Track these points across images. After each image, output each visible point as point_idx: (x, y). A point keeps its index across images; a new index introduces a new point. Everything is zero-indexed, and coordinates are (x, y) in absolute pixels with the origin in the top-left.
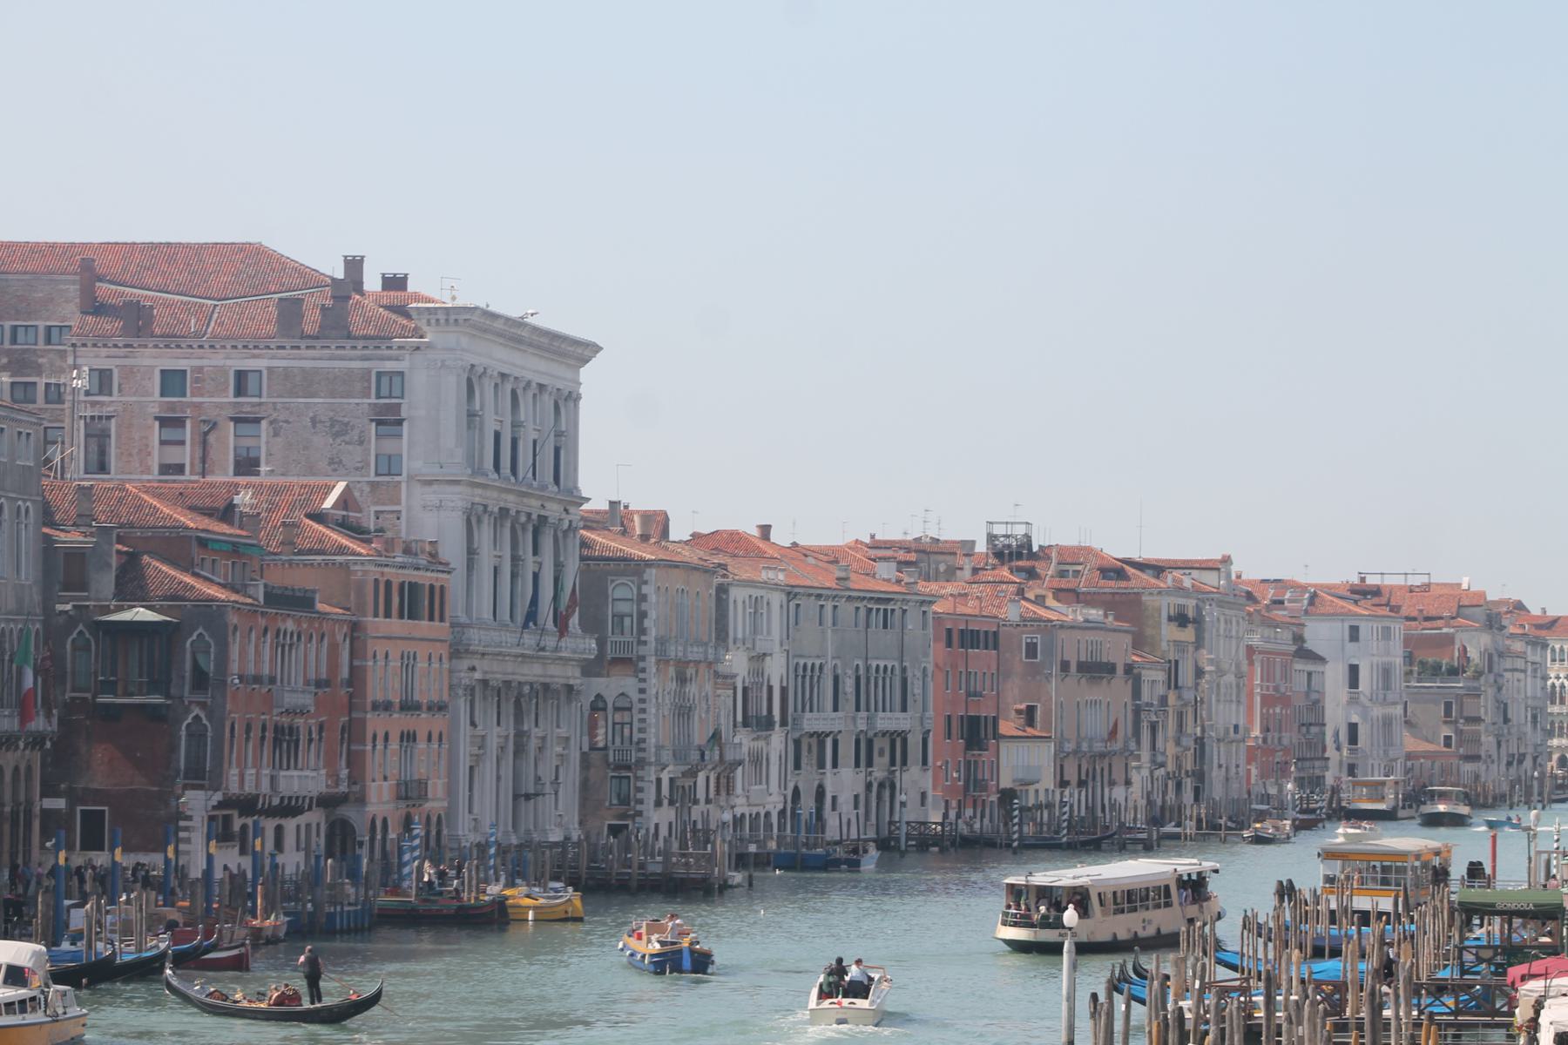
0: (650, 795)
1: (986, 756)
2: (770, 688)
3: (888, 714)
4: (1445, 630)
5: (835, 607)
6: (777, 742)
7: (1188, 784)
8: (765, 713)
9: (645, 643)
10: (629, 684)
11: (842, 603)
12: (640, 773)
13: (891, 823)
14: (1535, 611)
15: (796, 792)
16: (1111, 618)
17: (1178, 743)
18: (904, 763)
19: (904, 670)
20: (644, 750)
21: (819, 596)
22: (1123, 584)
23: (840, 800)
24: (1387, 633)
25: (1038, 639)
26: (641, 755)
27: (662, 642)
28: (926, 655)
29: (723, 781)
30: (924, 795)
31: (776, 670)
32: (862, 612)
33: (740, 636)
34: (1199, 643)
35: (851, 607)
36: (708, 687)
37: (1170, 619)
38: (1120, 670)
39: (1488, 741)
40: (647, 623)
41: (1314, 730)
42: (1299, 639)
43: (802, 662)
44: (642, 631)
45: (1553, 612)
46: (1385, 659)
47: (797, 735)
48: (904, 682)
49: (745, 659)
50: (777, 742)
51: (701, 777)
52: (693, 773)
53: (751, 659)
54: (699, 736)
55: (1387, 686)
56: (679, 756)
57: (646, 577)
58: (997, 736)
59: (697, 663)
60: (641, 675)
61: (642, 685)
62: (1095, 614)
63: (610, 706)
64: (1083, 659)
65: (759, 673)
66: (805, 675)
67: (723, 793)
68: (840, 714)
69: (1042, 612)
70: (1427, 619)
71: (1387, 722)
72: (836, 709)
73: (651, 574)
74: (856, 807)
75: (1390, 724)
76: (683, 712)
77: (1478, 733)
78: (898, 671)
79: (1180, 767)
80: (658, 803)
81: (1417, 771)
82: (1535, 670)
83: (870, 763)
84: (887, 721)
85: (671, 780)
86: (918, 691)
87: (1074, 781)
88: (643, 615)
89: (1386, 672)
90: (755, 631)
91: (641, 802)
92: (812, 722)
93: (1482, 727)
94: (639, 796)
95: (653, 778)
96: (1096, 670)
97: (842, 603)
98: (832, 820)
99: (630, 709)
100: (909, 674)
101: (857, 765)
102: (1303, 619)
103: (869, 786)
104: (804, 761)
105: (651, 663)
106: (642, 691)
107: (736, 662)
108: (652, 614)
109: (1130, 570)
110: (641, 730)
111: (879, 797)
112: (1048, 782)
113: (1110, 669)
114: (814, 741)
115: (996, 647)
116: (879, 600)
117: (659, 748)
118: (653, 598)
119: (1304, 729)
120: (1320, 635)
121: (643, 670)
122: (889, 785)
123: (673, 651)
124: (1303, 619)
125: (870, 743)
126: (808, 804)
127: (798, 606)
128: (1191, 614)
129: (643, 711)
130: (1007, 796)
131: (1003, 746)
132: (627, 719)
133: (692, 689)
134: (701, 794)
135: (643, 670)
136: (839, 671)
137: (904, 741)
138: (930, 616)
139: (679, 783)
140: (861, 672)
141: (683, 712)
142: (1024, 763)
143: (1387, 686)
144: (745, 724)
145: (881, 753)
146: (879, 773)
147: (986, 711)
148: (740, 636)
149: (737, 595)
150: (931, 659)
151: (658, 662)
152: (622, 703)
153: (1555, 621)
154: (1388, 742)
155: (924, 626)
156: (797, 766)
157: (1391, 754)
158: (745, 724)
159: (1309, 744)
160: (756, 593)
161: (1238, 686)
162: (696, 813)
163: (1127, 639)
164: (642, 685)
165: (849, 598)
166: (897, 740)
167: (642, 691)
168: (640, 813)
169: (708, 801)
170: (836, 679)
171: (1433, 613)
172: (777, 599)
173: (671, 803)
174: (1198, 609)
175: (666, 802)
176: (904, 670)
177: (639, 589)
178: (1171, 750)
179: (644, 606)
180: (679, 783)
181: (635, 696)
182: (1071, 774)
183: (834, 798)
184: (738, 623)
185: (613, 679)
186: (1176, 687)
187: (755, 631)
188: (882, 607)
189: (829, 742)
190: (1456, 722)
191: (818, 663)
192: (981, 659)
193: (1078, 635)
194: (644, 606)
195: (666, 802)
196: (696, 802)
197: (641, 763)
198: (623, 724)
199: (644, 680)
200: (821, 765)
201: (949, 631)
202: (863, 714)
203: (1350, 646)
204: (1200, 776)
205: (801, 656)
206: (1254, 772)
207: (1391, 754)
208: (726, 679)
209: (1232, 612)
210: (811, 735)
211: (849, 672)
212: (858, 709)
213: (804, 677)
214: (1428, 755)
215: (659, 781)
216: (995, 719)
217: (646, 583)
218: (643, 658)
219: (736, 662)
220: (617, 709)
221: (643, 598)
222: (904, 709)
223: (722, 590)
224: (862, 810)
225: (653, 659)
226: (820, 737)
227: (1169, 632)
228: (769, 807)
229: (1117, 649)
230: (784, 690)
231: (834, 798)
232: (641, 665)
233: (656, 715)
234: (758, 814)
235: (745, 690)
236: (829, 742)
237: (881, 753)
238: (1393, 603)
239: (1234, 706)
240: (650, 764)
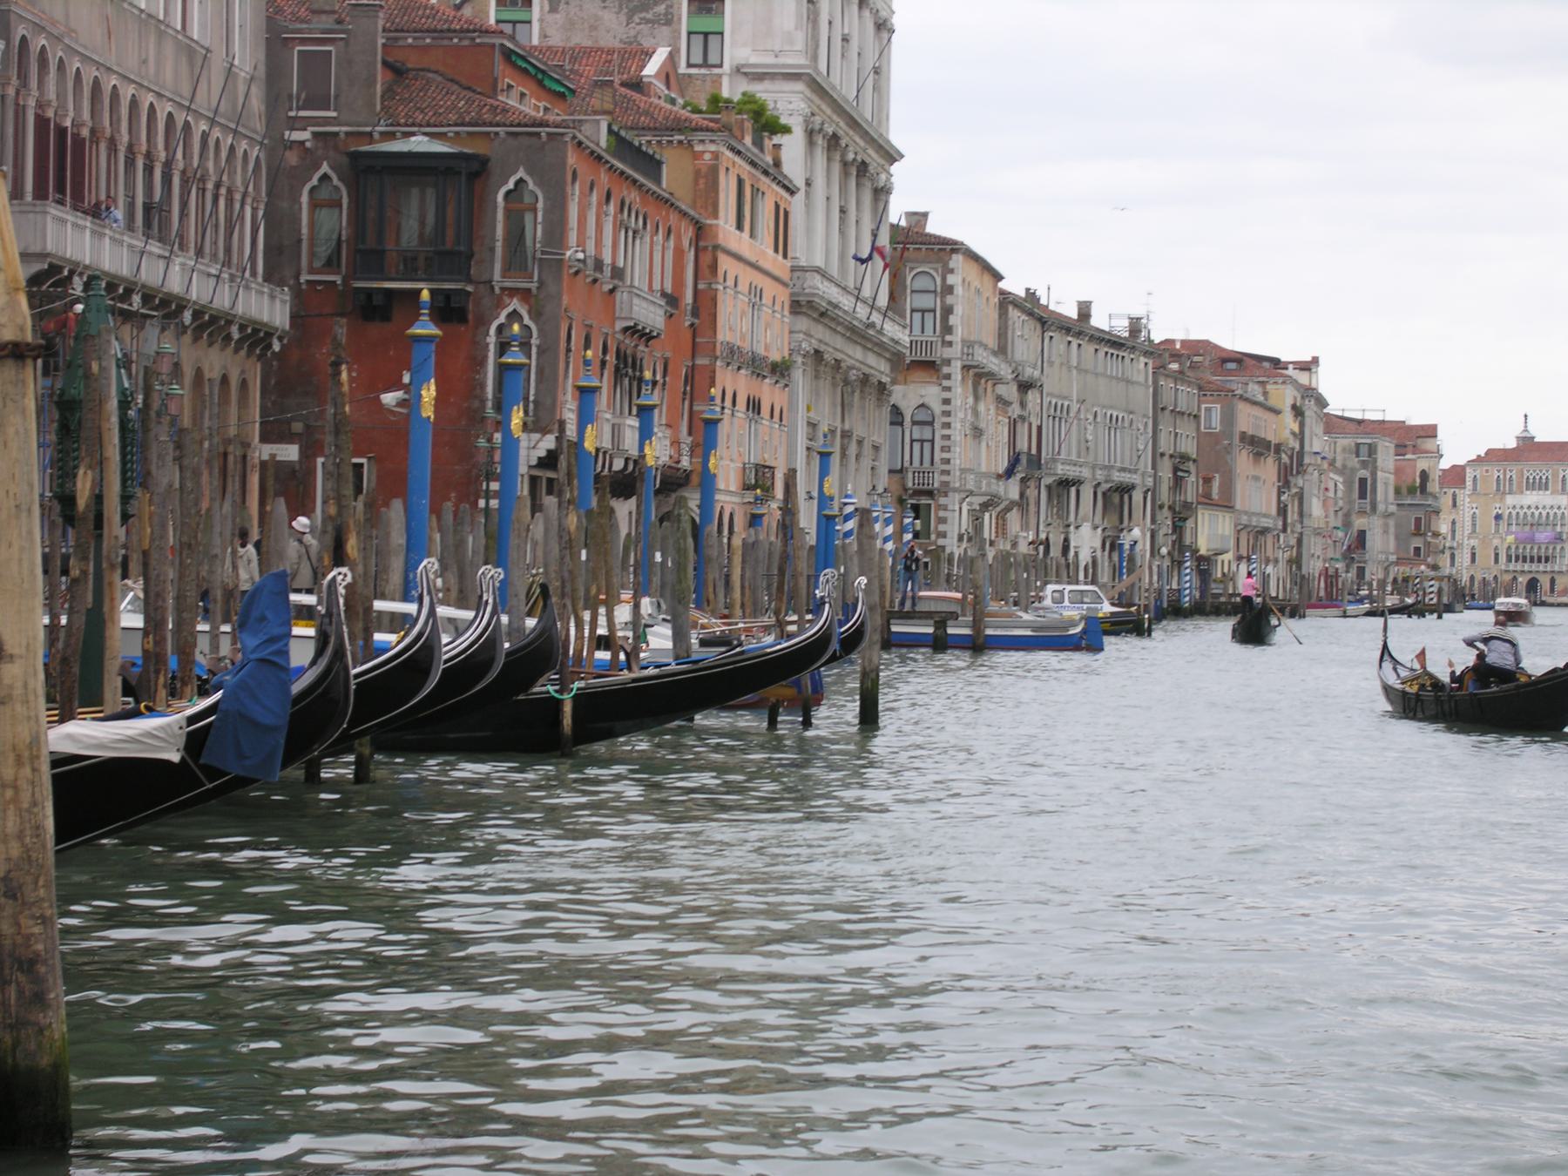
9: (950, 344)
10: (930, 393)
12: (942, 501)
26: (945, 478)
40: (953, 320)
44: (947, 329)
57: (952, 265)
60: (946, 383)
61: (946, 395)
63: (908, 420)
88: (948, 311)
91: (943, 535)
94: (941, 528)
99: (931, 424)
105: (955, 369)
106: (947, 402)
108: (959, 310)
110: (943, 449)
118: (959, 290)
121: (948, 377)
129: (947, 425)
132: (927, 435)
135: (948, 377)
152: (921, 417)
164: (946, 395)
167: (947, 402)
177: (944, 279)
179: (949, 300)
181: (937, 408)
185: (912, 387)
194: (949, 300)
197: (945, 489)
198: (922, 441)
199: (948, 389)
217: (952, 271)
218: (948, 362)
220: (914, 423)
221: (949, 290)
232: (945, 370)
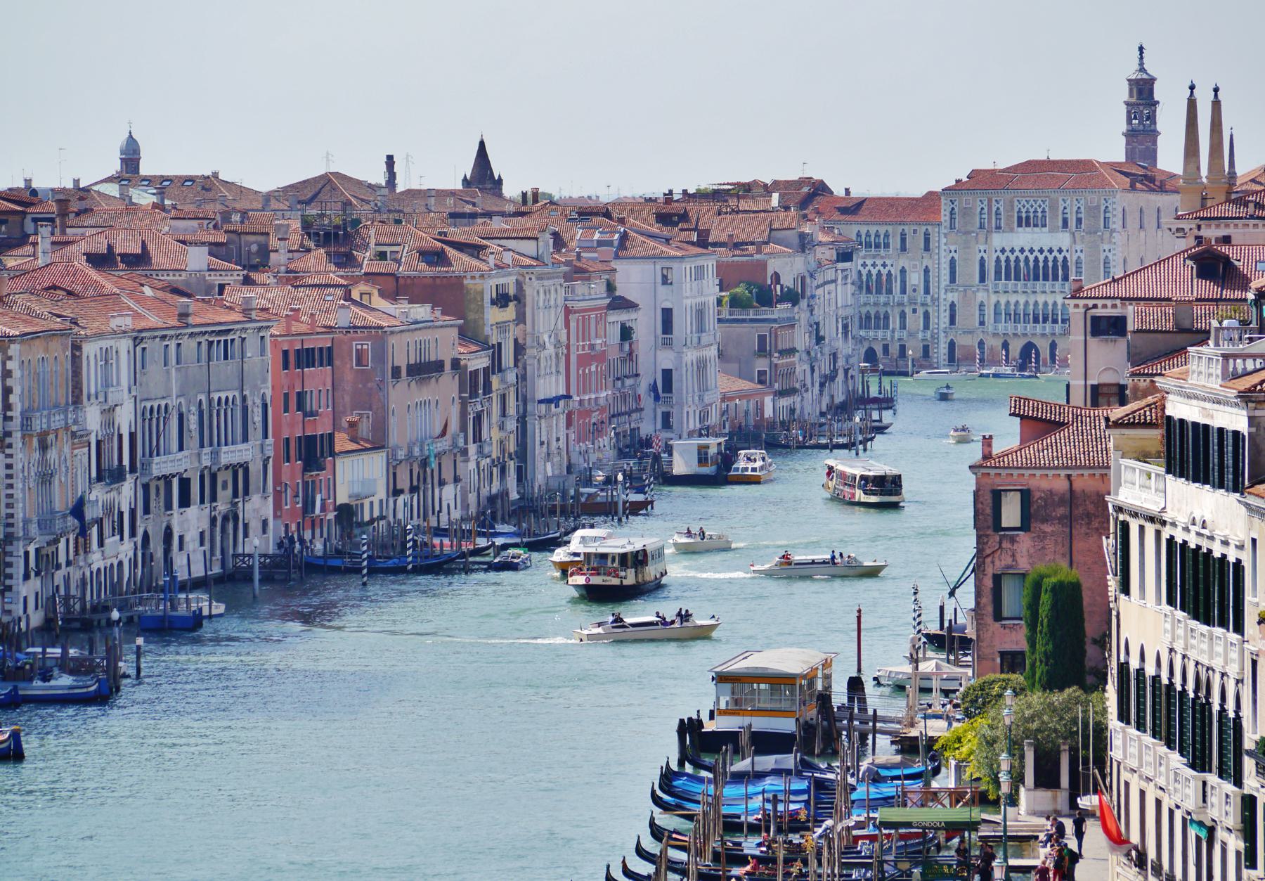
0: (18, 570)
1: (323, 475)
2: (120, 436)
3: (231, 448)
4: (757, 257)
5: (179, 345)
6: (126, 494)
7: (512, 466)
8: (116, 462)
9: (11, 418)
11: (185, 341)
13: (235, 556)
14: (839, 191)
15: (146, 536)
16: (438, 313)
17: (502, 428)
18: (246, 492)
19: (244, 398)
20: (12, 525)
21: (163, 337)
22: (440, 270)
23: (187, 539)
24: (700, 273)
25: (367, 346)
27: (26, 419)
28: (264, 381)
29: (81, 540)
30: (265, 523)
31: (125, 419)
32: (204, 346)
33: (93, 391)
34: (521, 318)
35: (193, 343)
36: (67, 449)
37: (493, 303)
38: (448, 366)
39: (802, 368)
40: (13, 399)
41: (629, 382)
42: (610, 287)
43: (148, 405)
45: (857, 193)
46: (699, 300)
47: (145, 480)
48: (245, 409)
49: (98, 412)
50: (126, 494)
51: (63, 540)
52: (56, 541)
53: (103, 412)
54: (61, 501)
55: (701, 329)
56: (44, 525)
57: (10, 353)
58: (332, 454)
59: (56, 431)
60: (8, 451)
61: (9, 461)
62: (422, 311)
64: (412, 362)
65: (109, 423)
66: (151, 417)
67: (81, 552)
68: (185, 453)
69: (373, 319)
70: (737, 245)
71: (702, 365)
72: (181, 448)
73: (14, 349)
74: (202, 544)
75: (705, 367)
76: (46, 478)
77: (793, 364)
78: (238, 401)
79: (503, 451)
80: (26, 577)
81: (732, 413)
82: (846, 277)
83: (214, 498)
84: (230, 455)
85: (37, 550)
86: (258, 418)
87: (406, 486)
89: (700, 313)
90: (107, 384)
91: (10, 577)
92: (160, 466)
93: (795, 359)
95: (22, 553)
96: (424, 370)
97: (185, 341)
98: (179, 561)
100: (249, 403)
101: (202, 501)
102: (614, 264)
103: (213, 521)
104: (153, 504)
107: (92, 418)
108: (17, 390)
109: (451, 252)
111: (223, 530)
112: (381, 493)
113: (438, 366)
114: (162, 483)
115: (330, 363)
116: (220, 333)
117: (26, 522)
118: (17, 374)
119: (619, 384)
120: (633, 278)
121: (10, 446)
122: (232, 517)
123: (38, 424)
124: (614, 264)
125: (214, 477)
126: (157, 549)
127: (144, 349)
128: (512, 291)
130: (346, 513)
131: (339, 462)
133: (52, 455)
134: (62, 559)
136: (184, 410)
137: (246, 470)
138: (268, 339)
139: (44, 552)
140: (204, 406)
141: (46, 478)
142: (358, 477)
143: (701, 329)
144: (100, 478)
145: (225, 487)
146: (222, 507)
147: (322, 427)
148: (93, 391)
149: (90, 350)
150: (270, 384)
151: (23, 437)
153: (861, 203)
154: (704, 388)
155: (263, 353)
156: (147, 510)
157: (707, 399)
158: (100, 478)
159: (624, 397)
160: (105, 344)
161: (557, 355)
162: (59, 576)
163: (454, 333)
164: (9, 461)
165: (192, 335)
166: (240, 471)
167: (9, 466)
168: (9, 588)
169: (69, 563)
170: (181, 416)
171: (744, 238)
172: (124, 345)
173: (37, 574)
174: (519, 285)
175: (33, 574)
176: (244, 398)
178: (496, 435)
179: (9, 382)
180: (44, 552)
182: (403, 483)
183: (181, 538)
184: (91, 381)
186: (500, 370)
187: (107, 384)
188: (222, 338)
189: (175, 482)
190: (771, 355)
191: (163, 403)
192: (317, 379)
193: (407, 337)
194: (9, 382)
195: (33, 574)
196: (58, 567)
199: (11, 456)
200: (169, 506)
201: (285, 353)
202: (207, 450)
203: (662, 290)
204: (522, 454)
205: (147, 400)
206: (572, 436)
207: (707, 399)
208: (78, 437)
209: (551, 282)
210: (159, 478)
211: (194, 409)
212: (202, 446)
213: (151, 420)
214: (744, 396)
215: (27, 554)
216: (331, 436)
217: (10, 358)
219: (92, 418)
222: (245, 439)
223: (77, 347)
224: (207, 547)
225: (19, 435)
226: (167, 479)
227: (494, 315)
228: (121, 557)
229: (445, 343)
230: (132, 436)
231: (181, 538)
233: (23, 490)
234: (112, 565)
235: (98, 443)
236: (175, 482)
237: (225, 487)
238: (700, 227)
239: (554, 378)
240: (18, 539)
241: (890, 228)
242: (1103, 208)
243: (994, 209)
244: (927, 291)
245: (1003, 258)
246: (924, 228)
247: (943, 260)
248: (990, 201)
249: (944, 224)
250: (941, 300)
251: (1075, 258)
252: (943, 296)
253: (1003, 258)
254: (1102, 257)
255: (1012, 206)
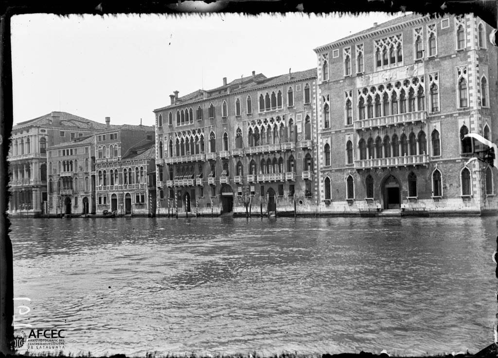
241: (281, 89)
242: (456, 28)
243: (357, 54)
244: (308, 138)
245: (365, 97)
246: (304, 84)
247: (319, 108)
248: (353, 48)
249: (319, 77)
250: (319, 144)
251: (430, 84)
252: (320, 141)
253: (365, 97)
254: (458, 79)
255: (372, 47)
